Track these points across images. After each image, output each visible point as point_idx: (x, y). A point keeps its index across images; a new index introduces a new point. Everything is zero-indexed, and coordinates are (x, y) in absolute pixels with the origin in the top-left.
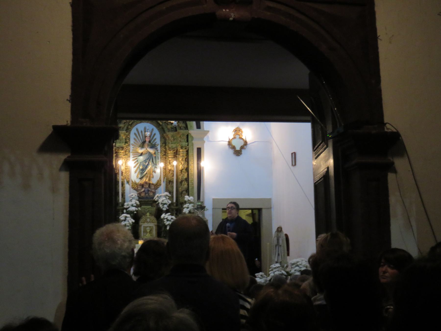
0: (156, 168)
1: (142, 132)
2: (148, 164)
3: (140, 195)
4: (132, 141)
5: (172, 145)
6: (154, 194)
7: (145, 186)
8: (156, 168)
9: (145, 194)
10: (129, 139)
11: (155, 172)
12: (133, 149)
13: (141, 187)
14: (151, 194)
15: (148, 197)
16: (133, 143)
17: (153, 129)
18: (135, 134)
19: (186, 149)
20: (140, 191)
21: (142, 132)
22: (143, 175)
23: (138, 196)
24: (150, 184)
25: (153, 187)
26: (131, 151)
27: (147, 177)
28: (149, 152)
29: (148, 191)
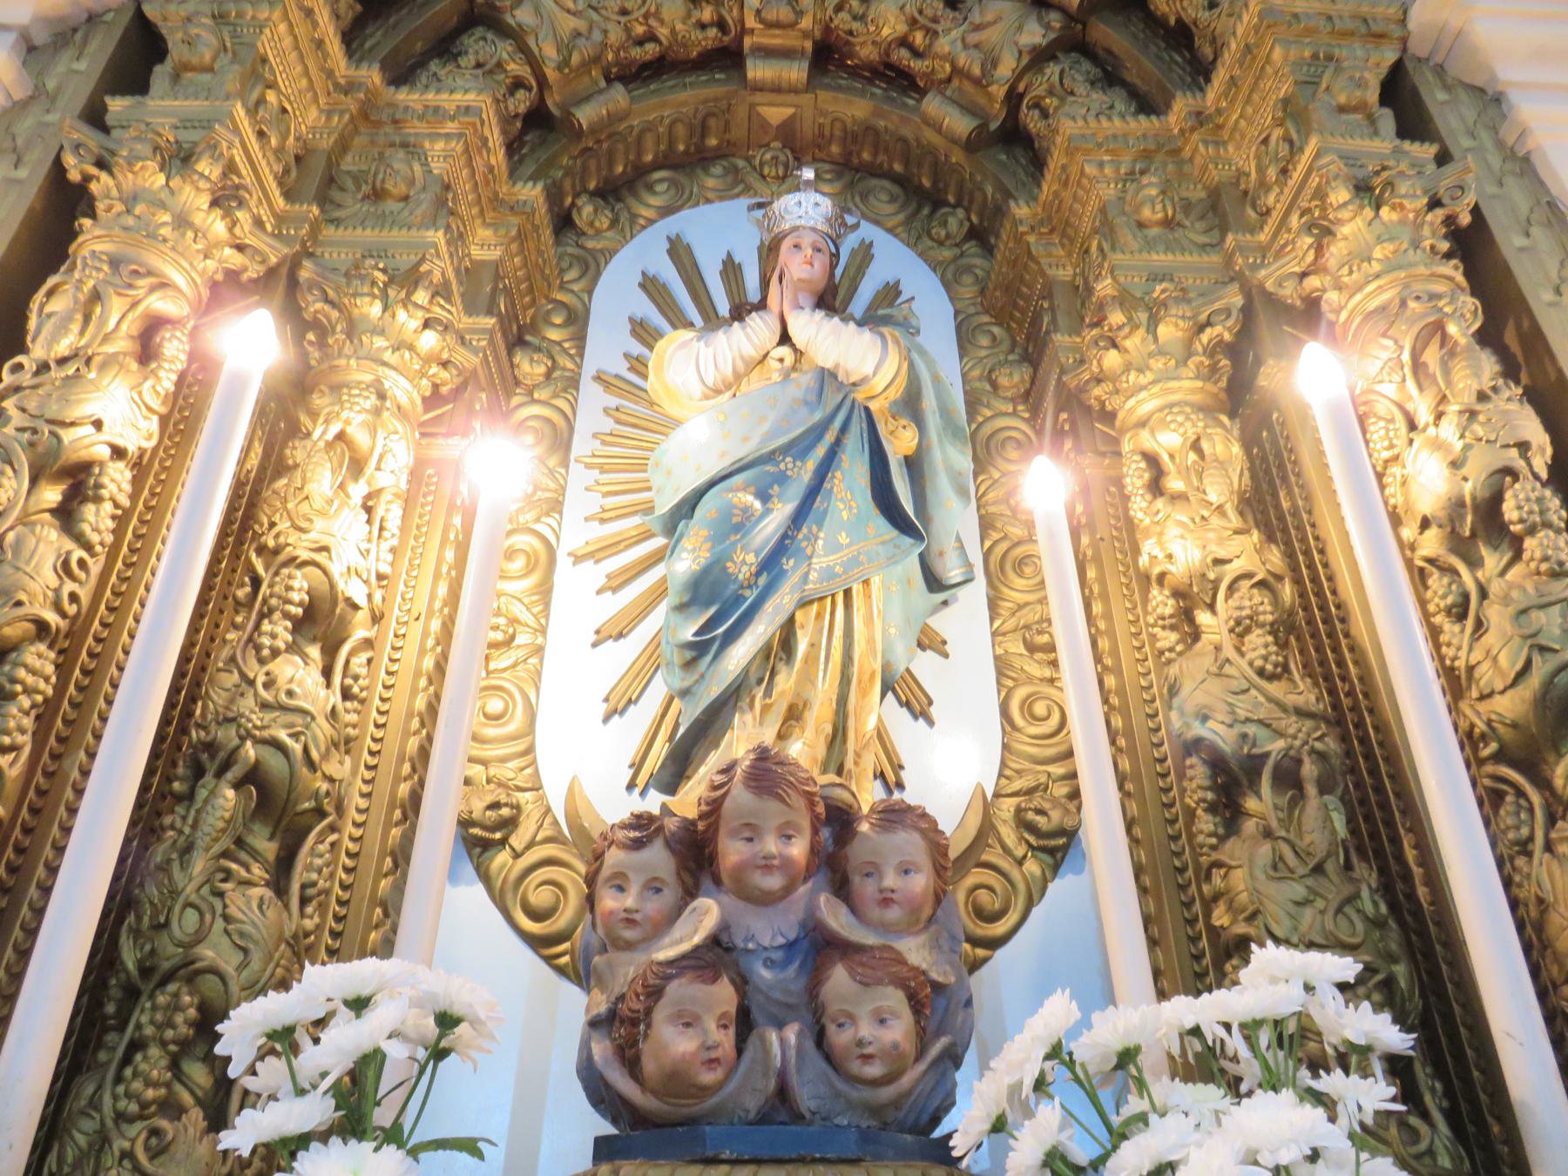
0: (929, 642)
1: (731, 270)
2: (798, 518)
3: (630, 1059)
4: (607, 345)
5: (1160, 259)
6: (941, 1017)
7: (732, 851)
8: (929, 642)
9: (744, 1024)
10: (578, 321)
11: (919, 708)
12: (608, 425)
13: (658, 858)
14: (877, 1023)
15: (806, 1097)
16: (622, 368)
17: (864, 254)
18: (651, 286)
19: (1435, 203)
20: (627, 970)
21: (731, 270)
22: (713, 690)
23: (600, 1094)
24: (839, 820)
25: (899, 870)
26: (582, 445)
27: (794, 715)
28: (827, 377)
29: (819, 948)
